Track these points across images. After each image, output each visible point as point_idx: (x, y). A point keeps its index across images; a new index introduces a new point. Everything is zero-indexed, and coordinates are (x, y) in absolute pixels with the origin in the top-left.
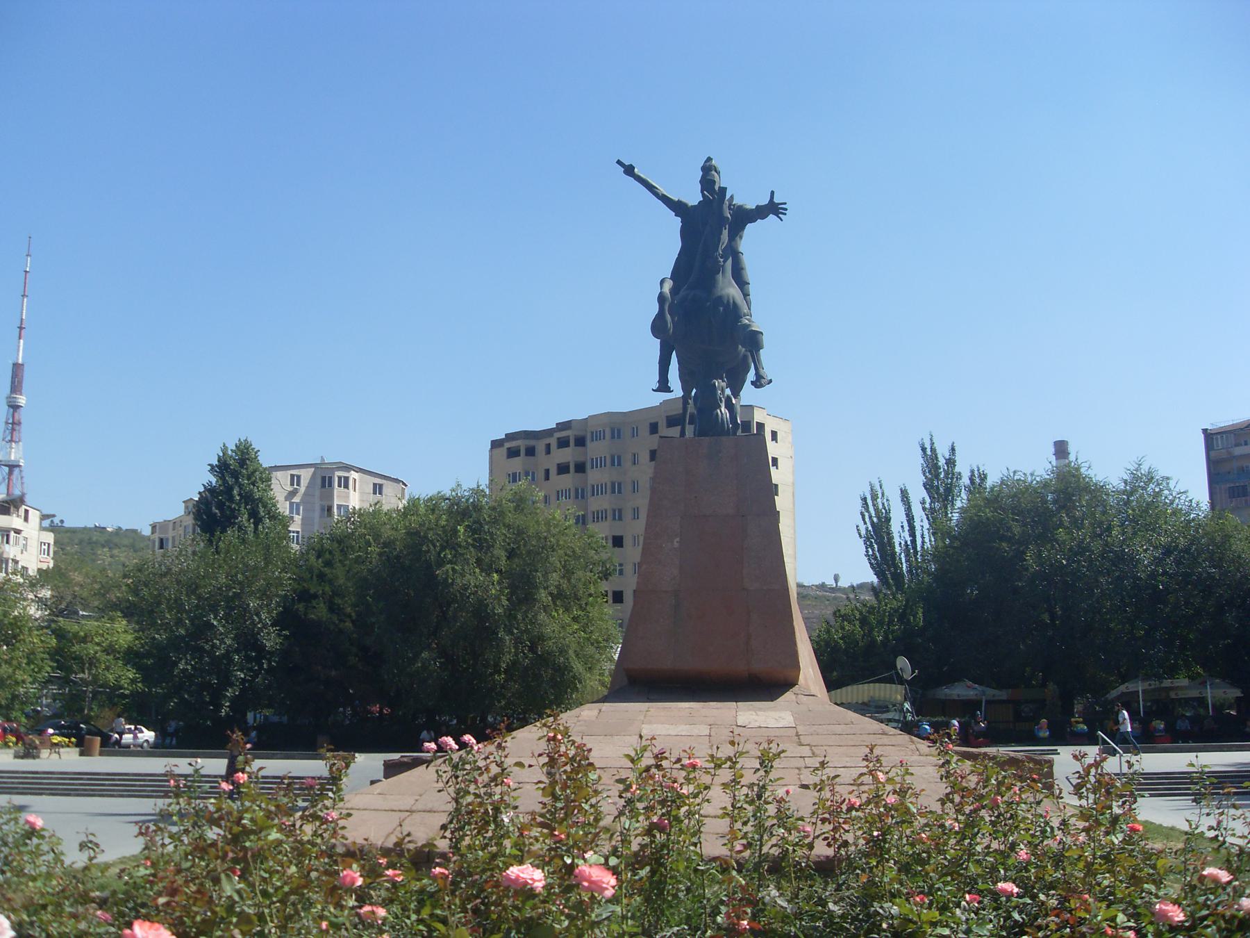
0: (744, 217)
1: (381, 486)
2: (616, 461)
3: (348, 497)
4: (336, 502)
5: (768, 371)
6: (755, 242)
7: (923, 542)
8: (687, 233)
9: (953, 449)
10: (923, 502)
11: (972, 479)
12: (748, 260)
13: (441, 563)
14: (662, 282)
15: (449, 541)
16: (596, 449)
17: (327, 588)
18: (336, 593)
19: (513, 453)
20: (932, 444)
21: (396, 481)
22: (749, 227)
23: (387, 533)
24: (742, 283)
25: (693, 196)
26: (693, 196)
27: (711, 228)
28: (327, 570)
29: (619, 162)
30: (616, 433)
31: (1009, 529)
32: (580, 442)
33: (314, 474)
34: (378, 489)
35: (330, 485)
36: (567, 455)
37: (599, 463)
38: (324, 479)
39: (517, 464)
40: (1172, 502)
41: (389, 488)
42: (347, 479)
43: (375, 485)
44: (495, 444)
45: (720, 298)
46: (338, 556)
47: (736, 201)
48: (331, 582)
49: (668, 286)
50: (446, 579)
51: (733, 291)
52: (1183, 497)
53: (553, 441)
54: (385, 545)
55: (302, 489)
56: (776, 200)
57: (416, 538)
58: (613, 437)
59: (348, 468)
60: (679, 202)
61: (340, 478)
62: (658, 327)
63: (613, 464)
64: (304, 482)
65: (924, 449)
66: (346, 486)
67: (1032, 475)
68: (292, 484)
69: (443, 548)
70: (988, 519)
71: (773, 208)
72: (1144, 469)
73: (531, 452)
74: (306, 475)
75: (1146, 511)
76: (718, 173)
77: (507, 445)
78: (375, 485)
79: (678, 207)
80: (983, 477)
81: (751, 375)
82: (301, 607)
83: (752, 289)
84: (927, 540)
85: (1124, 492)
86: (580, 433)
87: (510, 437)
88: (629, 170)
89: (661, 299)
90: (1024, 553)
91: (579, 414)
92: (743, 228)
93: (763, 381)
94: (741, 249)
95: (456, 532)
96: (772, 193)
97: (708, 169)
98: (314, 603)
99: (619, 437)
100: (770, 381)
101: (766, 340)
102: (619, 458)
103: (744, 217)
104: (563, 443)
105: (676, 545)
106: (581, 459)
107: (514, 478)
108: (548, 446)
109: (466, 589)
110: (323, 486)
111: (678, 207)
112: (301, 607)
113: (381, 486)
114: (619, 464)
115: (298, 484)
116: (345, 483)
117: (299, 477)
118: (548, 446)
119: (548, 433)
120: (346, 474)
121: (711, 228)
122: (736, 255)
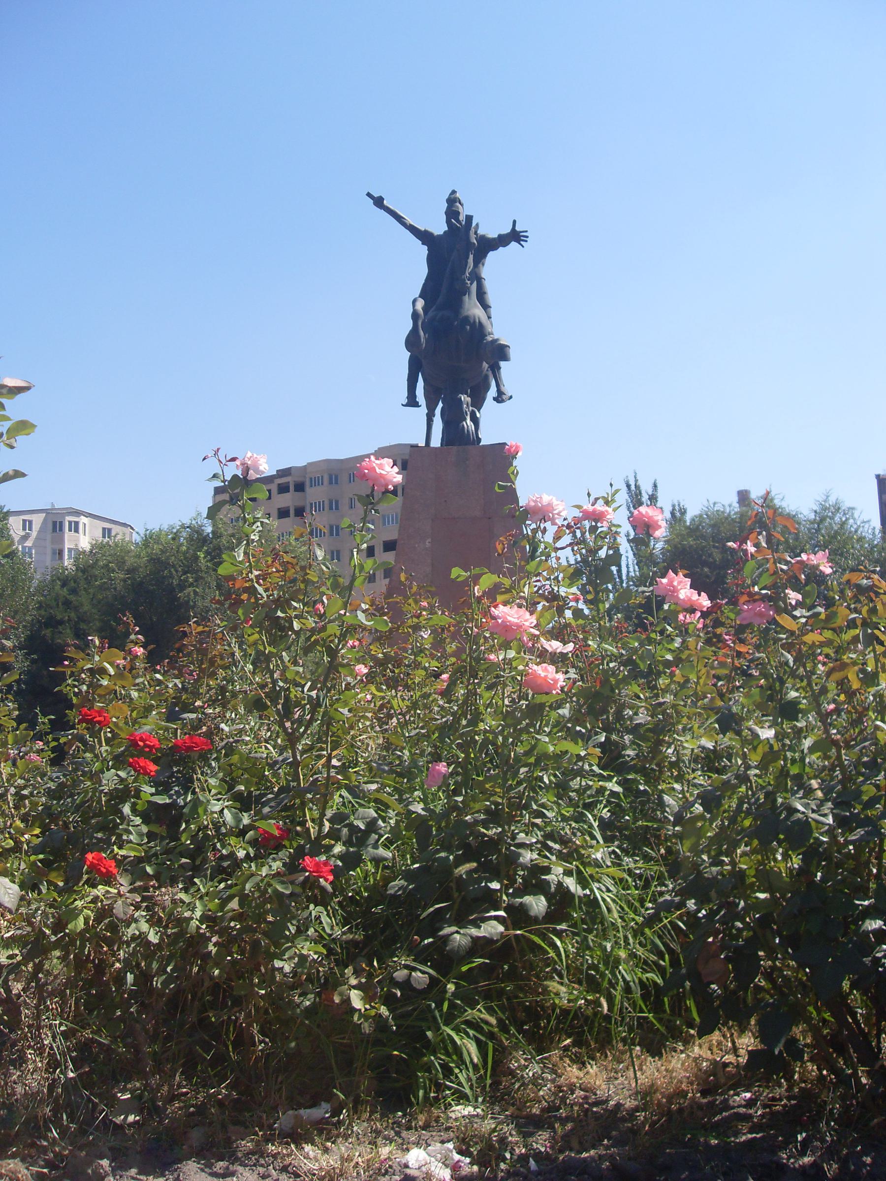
0: (488, 245)
1: (110, 530)
2: (334, 505)
4: (67, 545)
5: (507, 389)
6: (495, 268)
7: (628, 572)
8: (432, 260)
9: (655, 486)
10: (628, 535)
11: (673, 514)
12: (488, 285)
13: (182, 586)
14: (414, 302)
15: (190, 565)
16: (314, 494)
17: (73, 615)
18: (81, 619)
20: (636, 481)
21: (125, 525)
22: (491, 254)
23: (130, 561)
24: (486, 307)
25: (439, 227)
26: (439, 227)
27: (455, 256)
28: (72, 598)
29: (369, 195)
30: (334, 479)
31: (710, 555)
32: (300, 487)
33: (45, 520)
34: (106, 532)
35: (61, 529)
36: (287, 500)
37: (319, 507)
38: (55, 523)
40: (856, 531)
42: (77, 523)
43: (104, 529)
45: (467, 318)
46: (83, 584)
47: (481, 232)
48: (76, 609)
49: (420, 304)
50: (188, 602)
51: (477, 311)
52: (867, 526)
53: (274, 487)
54: (129, 571)
55: (34, 534)
56: (518, 229)
57: (158, 563)
58: (331, 483)
59: (78, 513)
60: (426, 231)
61: (70, 523)
62: (411, 342)
63: (331, 508)
64: (36, 527)
65: (628, 486)
66: (77, 531)
67: (730, 506)
68: (24, 529)
69: (185, 573)
70: (691, 546)
71: (516, 236)
72: (832, 500)
74: (37, 520)
75: (834, 537)
76: (462, 205)
78: (104, 529)
79: (424, 236)
80: (683, 512)
81: (492, 392)
82: (47, 632)
83: (493, 311)
84: (631, 569)
85: (813, 522)
86: (300, 479)
88: (379, 202)
89: (415, 316)
90: (725, 576)
91: (300, 462)
92: (485, 256)
93: (504, 397)
94: (483, 276)
95: (197, 558)
96: (514, 222)
97: (452, 201)
98: (60, 628)
99: (336, 483)
100: (511, 397)
101: (512, 353)
102: (337, 502)
103: (488, 245)
104: (283, 489)
105: (428, 545)
106: (300, 504)
109: (207, 612)
110: (54, 530)
111: (424, 236)
112: (47, 632)
113: (110, 530)
114: (337, 508)
115: (30, 529)
117: (30, 522)
120: (76, 519)
121: (455, 256)
122: (479, 280)
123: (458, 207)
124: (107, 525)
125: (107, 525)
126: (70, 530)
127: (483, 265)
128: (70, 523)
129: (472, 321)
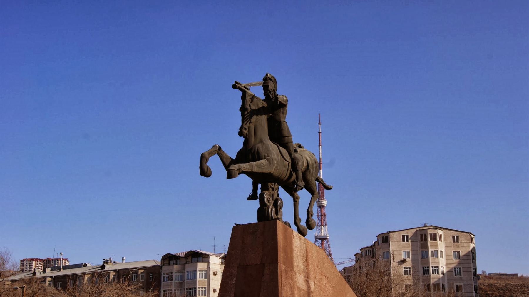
1: (457, 237)
3: (436, 246)
34: (456, 239)
35: (426, 239)
38: (422, 236)
41: (463, 239)
42: (435, 235)
43: (454, 237)
61: (431, 235)
76: (274, 81)
88: (234, 87)
97: (266, 79)
110: (422, 240)
116: (434, 237)
123: (268, 83)
124: (455, 234)
125: (455, 234)
126: (431, 239)
127: (284, 113)
128: (431, 235)
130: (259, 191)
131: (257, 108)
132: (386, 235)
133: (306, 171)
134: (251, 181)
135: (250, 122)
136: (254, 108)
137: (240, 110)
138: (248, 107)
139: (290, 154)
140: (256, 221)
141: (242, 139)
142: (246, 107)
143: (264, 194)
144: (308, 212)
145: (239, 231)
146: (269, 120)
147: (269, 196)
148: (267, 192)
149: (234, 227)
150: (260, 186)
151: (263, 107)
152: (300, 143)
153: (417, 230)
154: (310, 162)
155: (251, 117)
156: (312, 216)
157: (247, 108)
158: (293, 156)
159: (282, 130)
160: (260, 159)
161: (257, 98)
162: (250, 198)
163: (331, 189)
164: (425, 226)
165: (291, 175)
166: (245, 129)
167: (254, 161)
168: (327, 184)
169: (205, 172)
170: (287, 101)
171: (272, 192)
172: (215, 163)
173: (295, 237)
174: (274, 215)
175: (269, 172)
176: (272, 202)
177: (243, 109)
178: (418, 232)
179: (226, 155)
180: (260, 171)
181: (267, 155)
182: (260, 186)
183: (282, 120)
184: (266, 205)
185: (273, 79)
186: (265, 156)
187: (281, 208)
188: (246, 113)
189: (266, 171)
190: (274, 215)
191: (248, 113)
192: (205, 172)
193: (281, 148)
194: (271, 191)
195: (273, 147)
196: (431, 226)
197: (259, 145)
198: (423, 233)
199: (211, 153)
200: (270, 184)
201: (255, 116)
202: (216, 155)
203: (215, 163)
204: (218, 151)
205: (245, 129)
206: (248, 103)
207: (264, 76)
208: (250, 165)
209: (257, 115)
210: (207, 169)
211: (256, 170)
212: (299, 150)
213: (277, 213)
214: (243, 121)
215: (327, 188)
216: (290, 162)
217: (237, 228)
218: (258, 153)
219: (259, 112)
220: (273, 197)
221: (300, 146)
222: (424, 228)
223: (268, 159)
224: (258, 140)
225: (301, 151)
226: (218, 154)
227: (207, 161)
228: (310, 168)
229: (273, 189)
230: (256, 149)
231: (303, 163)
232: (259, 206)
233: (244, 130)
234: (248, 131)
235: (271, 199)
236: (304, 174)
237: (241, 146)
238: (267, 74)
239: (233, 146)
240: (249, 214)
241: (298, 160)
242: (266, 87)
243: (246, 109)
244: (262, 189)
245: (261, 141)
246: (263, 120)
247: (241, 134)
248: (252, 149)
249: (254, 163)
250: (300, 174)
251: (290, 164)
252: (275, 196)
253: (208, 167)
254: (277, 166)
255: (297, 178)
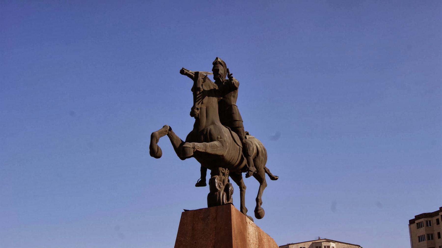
19: (419, 226)
39: (422, 231)
44: (411, 222)
73: (429, 224)
77: (417, 222)
87: (418, 217)
88: (182, 72)
97: (216, 64)
107: (421, 239)
108: (438, 220)
118: (438, 220)
119: (436, 213)
123: (218, 67)
127: (235, 97)
129: (205, 133)
130: (208, 177)
131: (208, 89)
132: (286, 247)
133: (255, 158)
134: (199, 165)
135: (202, 103)
136: (206, 89)
137: (192, 90)
138: (201, 87)
139: (241, 139)
140: (206, 206)
141: (193, 120)
142: (198, 86)
143: (214, 179)
144: (257, 200)
145: (189, 218)
146: (220, 103)
147: (220, 181)
148: (217, 176)
149: (183, 213)
150: (209, 172)
151: (215, 89)
152: (248, 131)
153: (313, 243)
154: (260, 149)
155: (203, 98)
156: (261, 204)
157: (199, 88)
158: (244, 141)
159: (233, 113)
160: (212, 140)
161: (209, 79)
162: (198, 185)
163: (277, 179)
164: (319, 239)
165: (242, 159)
166: (198, 109)
167: (208, 142)
168: (274, 174)
169: (155, 153)
170: (238, 84)
171: (223, 177)
172: (164, 144)
173: (248, 224)
174: (225, 201)
175: (221, 154)
176: (223, 187)
177: (195, 89)
178: (314, 244)
179: (176, 136)
180: (213, 153)
181: (219, 137)
182: (209, 172)
183: (233, 104)
184: (217, 190)
185: (223, 63)
186: (217, 138)
187: (232, 194)
188: (198, 93)
189: (219, 153)
190: (225, 201)
191: (200, 93)
192: (155, 153)
193: (232, 132)
194: (222, 176)
195: (225, 130)
196: (325, 239)
197: (212, 127)
198: (318, 245)
199: (162, 134)
200: (221, 169)
201: (207, 97)
202: (167, 135)
203: (164, 144)
204: (169, 132)
205: (198, 109)
206: (201, 83)
207: (213, 60)
208: (204, 145)
209: (209, 96)
210: (158, 149)
211: (209, 151)
212: (247, 137)
213: (228, 198)
214: (195, 102)
215: (273, 178)
216: (242, 146)
217: (186, 214)
218: (210, 134)
219: (211, 93)
220: (223, 182)
221: (248, 134)
222: (319, 241)
223: (221, 142)
224: (210, 122)
225: (250, 138)
226: (168, 135)
227: (157, 141)
228: (260, 154)
229: (224, 174)
230: (209, 131)
231: (253, 149)
232: (209, 192)
233: (196, 110)
234: (201, 112)
235: (222, 184)
236: (254, 160)
237: (191, 129)
238: (217, 58)
239: (184, 127)
240: (199, 200)
241: (249, 144)
242: (215, 71)
243: (199, 89)
244: (212, 174)
245: (213, 123)
246: (214, 102)
247: (192, 114)
248: (203, 130)
249: (208, 144)
250: (251, 159)
251: (241, 149)
252: (226, 182)
253: (158, 148)
254: (229, 150)
255: (248, 163)
